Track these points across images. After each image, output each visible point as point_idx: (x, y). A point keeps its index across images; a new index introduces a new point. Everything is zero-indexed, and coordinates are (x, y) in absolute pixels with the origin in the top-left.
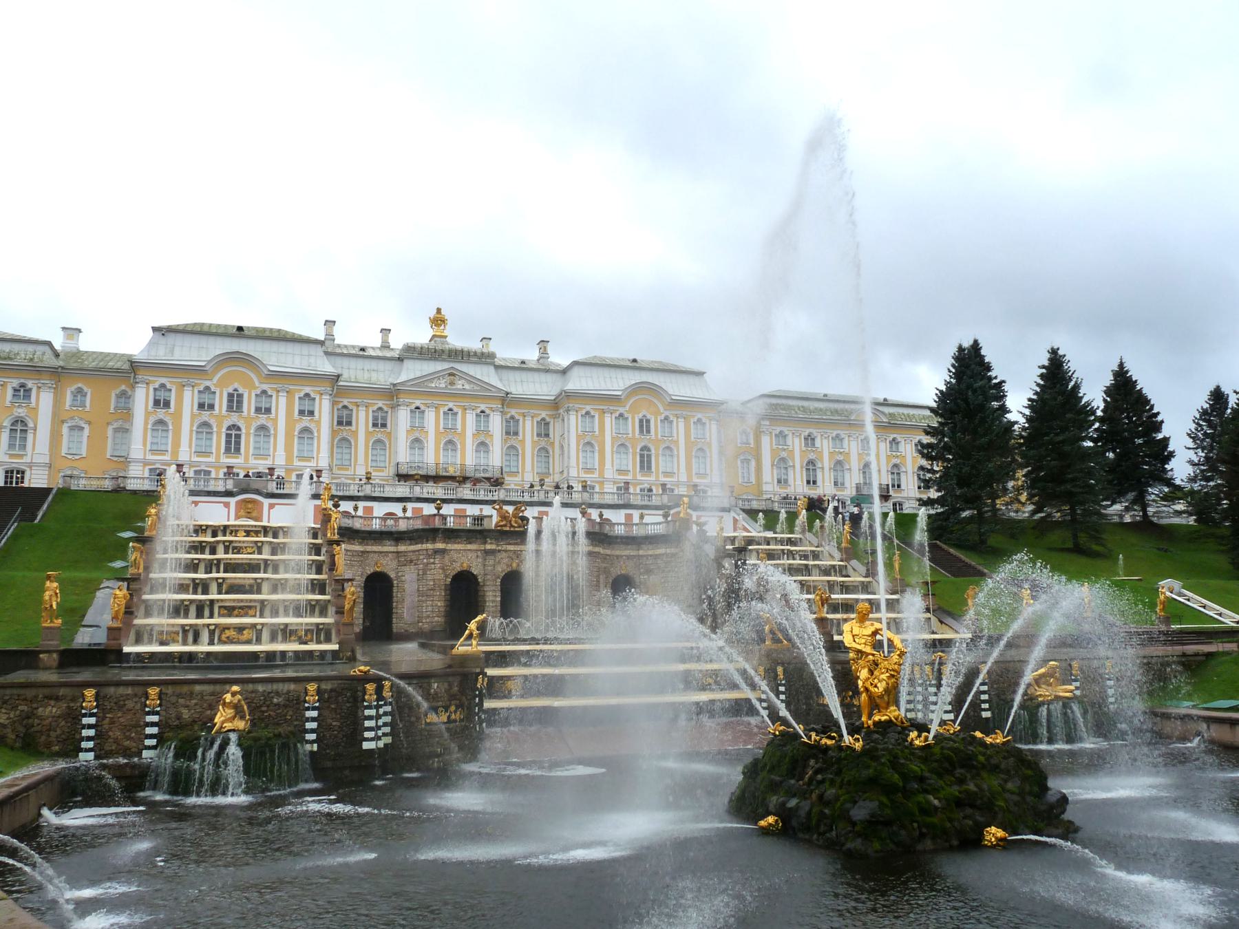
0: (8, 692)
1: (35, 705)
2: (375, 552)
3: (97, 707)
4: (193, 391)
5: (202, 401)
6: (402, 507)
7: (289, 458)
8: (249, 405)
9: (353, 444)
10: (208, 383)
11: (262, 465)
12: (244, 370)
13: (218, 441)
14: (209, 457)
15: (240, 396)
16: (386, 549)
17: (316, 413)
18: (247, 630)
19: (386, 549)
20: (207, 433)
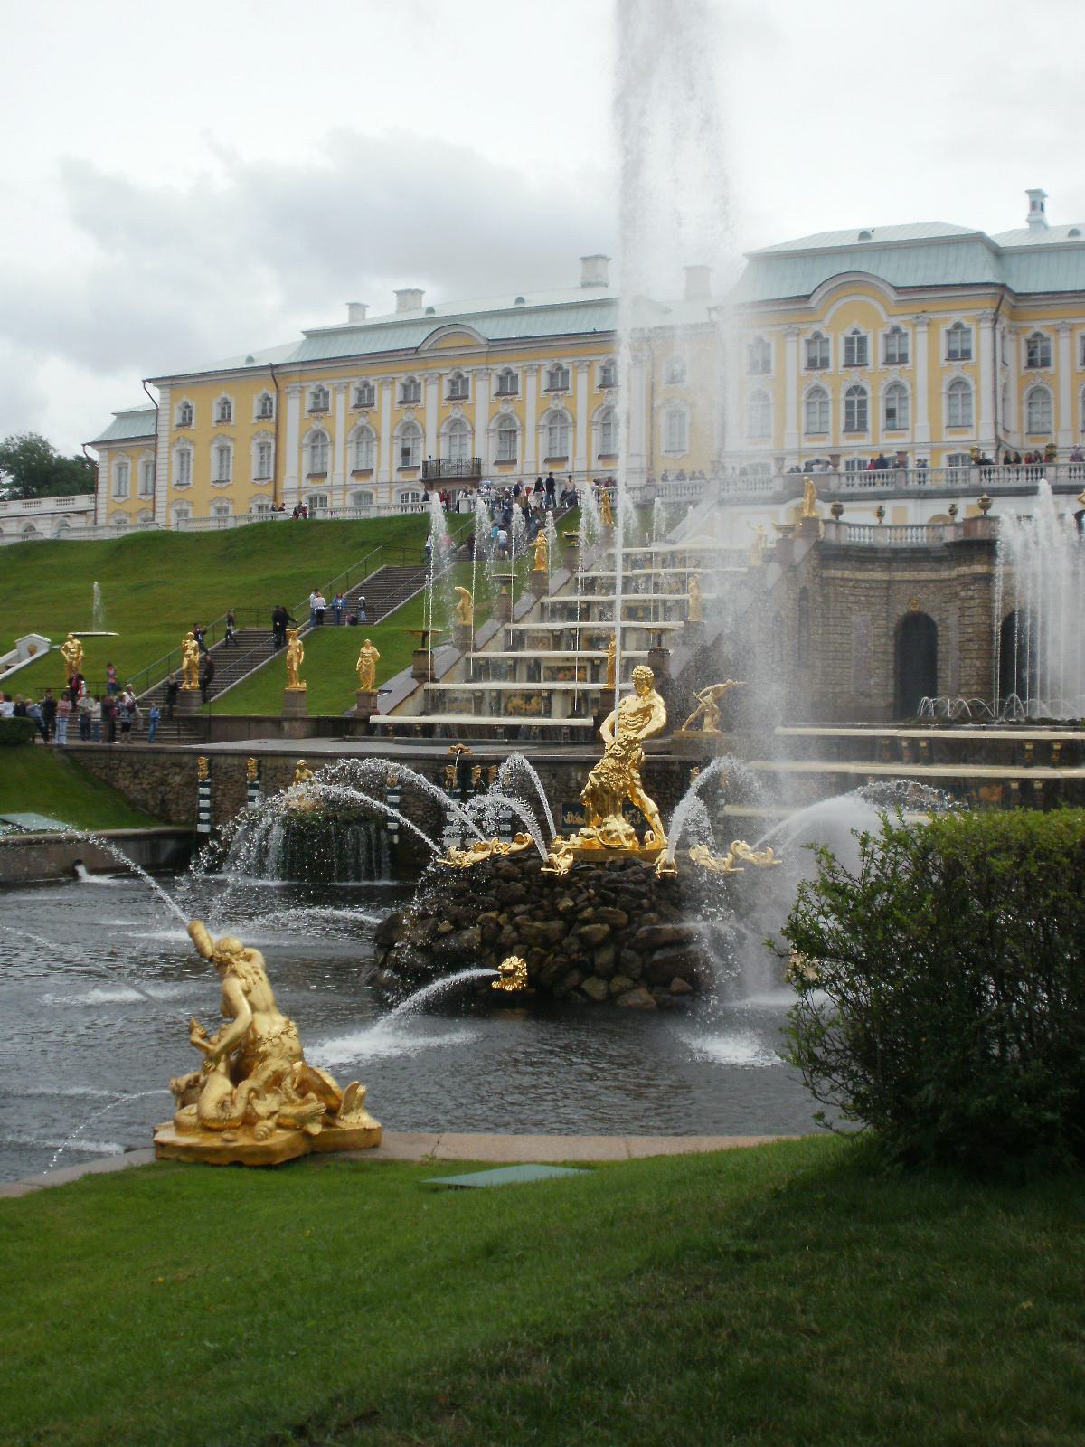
0: (147, 756)
1: (165, 772)
2: (909, 581)
3: (209, 776)
4: (798, 341)
5: (812, 356)
6: (949, 507)
7: (935, 431)
8: (876, 351)
9: (1052, 395)
10: (816, 327)
11: (889, 444)
12: (862, 298)
13: (837, 414)
14: (824, 439)
15: (862, 340)
16: (923, 576)
17: (973, 355)
18: (535, 698)
19: (923, 576)
20: (821, 403)
